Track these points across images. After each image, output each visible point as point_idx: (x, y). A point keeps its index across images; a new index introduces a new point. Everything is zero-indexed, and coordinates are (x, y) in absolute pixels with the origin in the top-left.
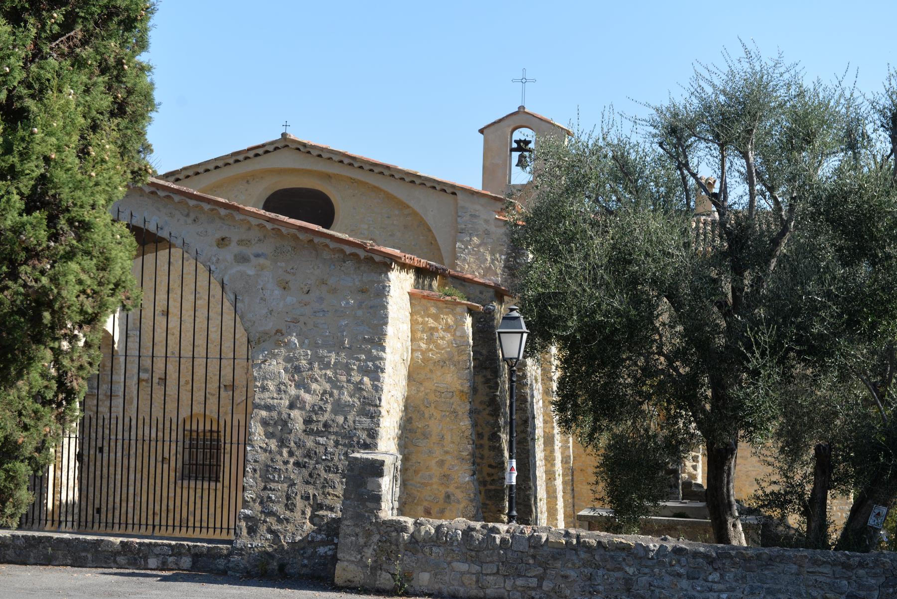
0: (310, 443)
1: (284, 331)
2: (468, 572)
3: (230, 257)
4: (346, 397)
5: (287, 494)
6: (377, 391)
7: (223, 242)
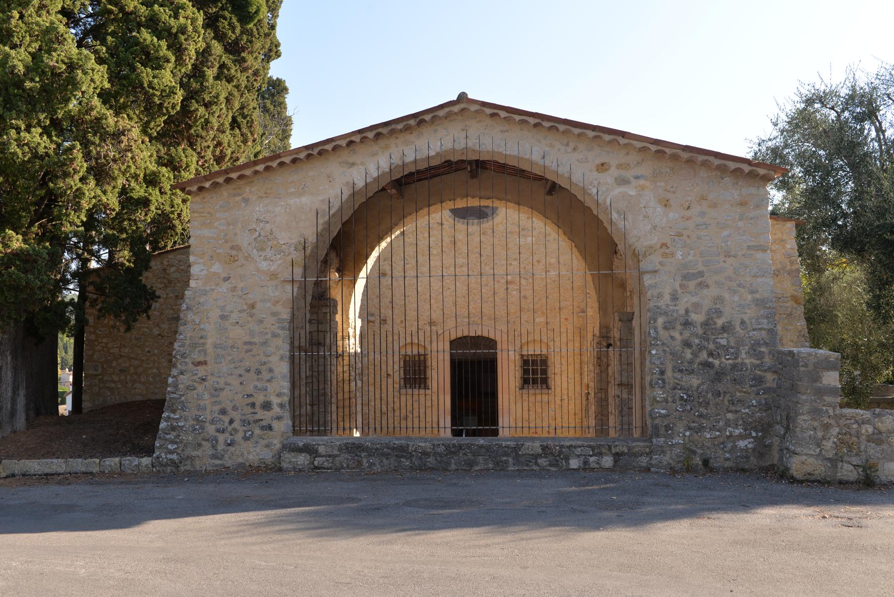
7: (602, 167)
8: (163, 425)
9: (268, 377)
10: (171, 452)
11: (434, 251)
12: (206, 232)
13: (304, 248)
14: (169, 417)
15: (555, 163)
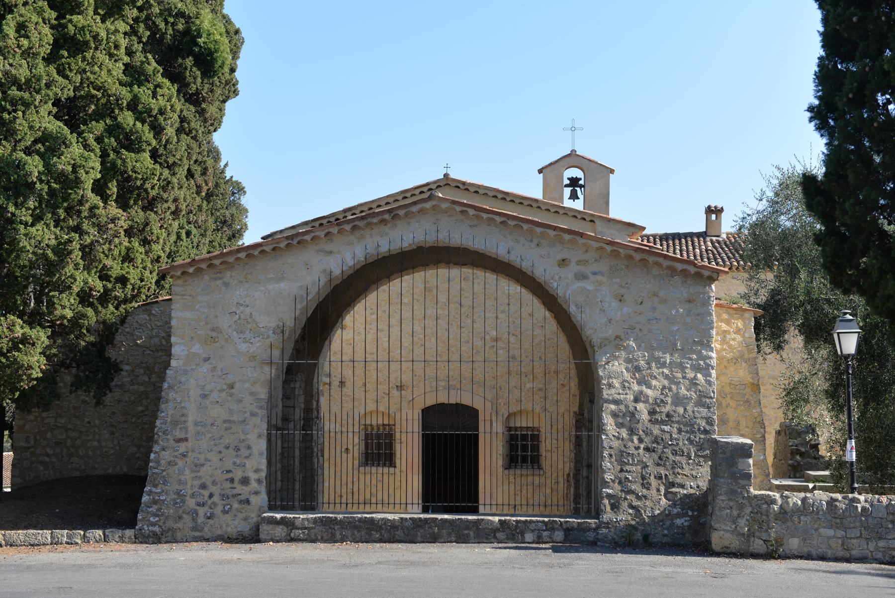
0: (656, 431)
1: (622, 337)
2: (834, 537)
3: (570, 276)
4: (683, 391)
5: (642, 475)
6: (710, 385)
7: (563, 263)
8: (145, 498)
9: (246, 453)
10: (153, 524)
11: (405, 300)
12: (188, 314)
13: (283, 332)
14: (151, 491)
15: (519, 258)
